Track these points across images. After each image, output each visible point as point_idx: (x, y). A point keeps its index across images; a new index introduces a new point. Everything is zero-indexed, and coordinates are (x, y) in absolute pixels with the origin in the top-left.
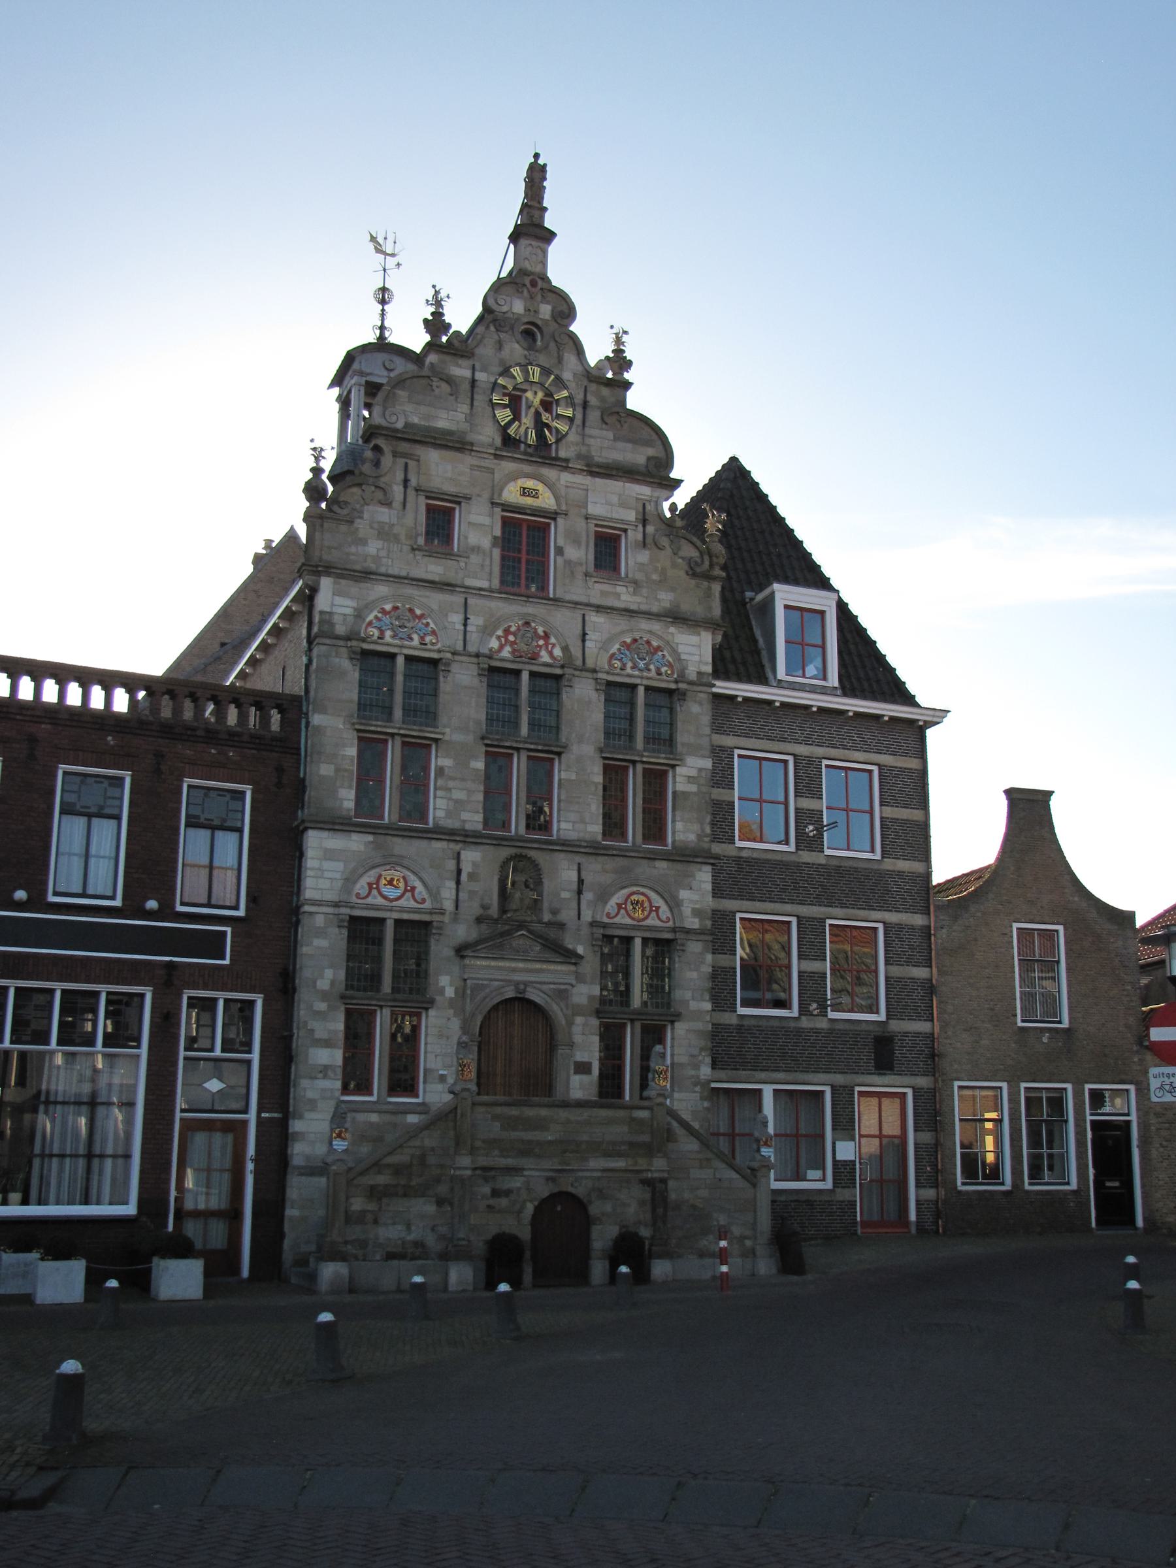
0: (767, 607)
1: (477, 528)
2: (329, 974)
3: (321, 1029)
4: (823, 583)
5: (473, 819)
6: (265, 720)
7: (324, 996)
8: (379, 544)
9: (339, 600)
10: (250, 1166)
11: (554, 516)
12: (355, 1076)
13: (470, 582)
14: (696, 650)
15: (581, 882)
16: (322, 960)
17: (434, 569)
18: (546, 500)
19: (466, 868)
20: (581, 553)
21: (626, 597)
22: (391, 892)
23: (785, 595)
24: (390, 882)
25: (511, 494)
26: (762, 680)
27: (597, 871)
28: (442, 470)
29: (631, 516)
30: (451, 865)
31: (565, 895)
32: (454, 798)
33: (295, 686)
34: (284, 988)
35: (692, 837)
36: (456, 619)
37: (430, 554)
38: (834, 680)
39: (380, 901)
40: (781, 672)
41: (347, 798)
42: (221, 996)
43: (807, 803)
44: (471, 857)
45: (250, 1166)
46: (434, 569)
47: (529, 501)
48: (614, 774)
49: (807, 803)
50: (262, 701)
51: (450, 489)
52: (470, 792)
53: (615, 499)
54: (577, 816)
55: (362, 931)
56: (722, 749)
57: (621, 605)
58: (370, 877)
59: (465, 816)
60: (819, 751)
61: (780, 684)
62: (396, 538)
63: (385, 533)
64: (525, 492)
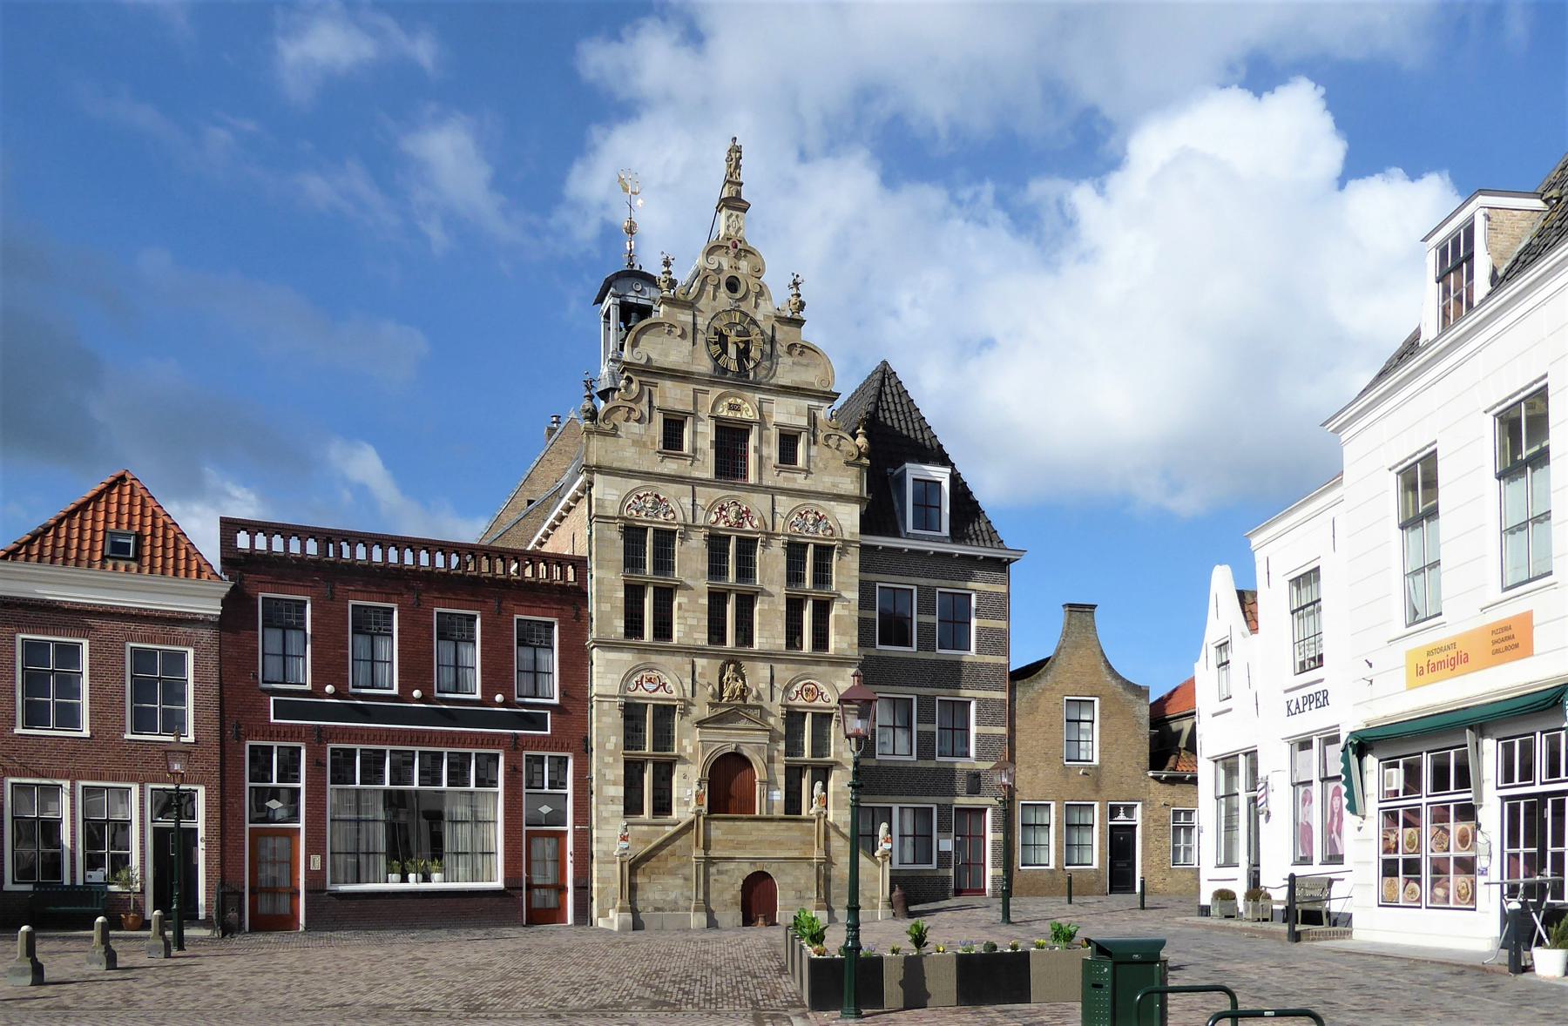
0: (901, 479)
1: (701, 437)
2: (613, 739)
3: (610, 775)
4: (942, 459)
5: (702, 638)
6: (564, 574)
7: (611, 753)
8: (633, 450)
9: (608, 491)
10: (569, 858)
11: (750, 424)
12: (632, 806)
13: (696, 474)
14: (848, 518)
15: (772, 677)
16: (605, 729)
17: (671, 467)
18: (748, 413)
19: (698, 670)
20: (773, 452)
21: (800, 481)
22: (651, 687)
23: (914, 471)
24: (650, 680)
25: (723, 411)
26: (896, 533)
27: (784, 672)
28: (674, 395)
29: (804, 422)
30: (689, 668)
31: (762, 686)
32: (689, 622)
33: (581, 551)
34: (583, 750)
35: (845, 646)
36: (687, 501)
37: (666, 456)
38: (946, 531)
39: (644, 693)
40: (910, 528)
41: (619, 625)
42: (547, 754)
43: (926, 619)
44: (701, 662)
45: (569, 858)
46: (671, 467)
47: (731, 414)
48: (794, 607)
49: (926, 619)
50: (560, 560)
51: (679, 407)
52: (699, 620)
53: (793, 410)
54: (768, 631)
55: (632, 713)
56: (868, 582)
57: (797, 486)
58: (638, 678)
59: (696, 635)
60: (934, 582)
61: (909, 536)
62: (645, 445)
63: (638, 443)
64: (732, 407)
